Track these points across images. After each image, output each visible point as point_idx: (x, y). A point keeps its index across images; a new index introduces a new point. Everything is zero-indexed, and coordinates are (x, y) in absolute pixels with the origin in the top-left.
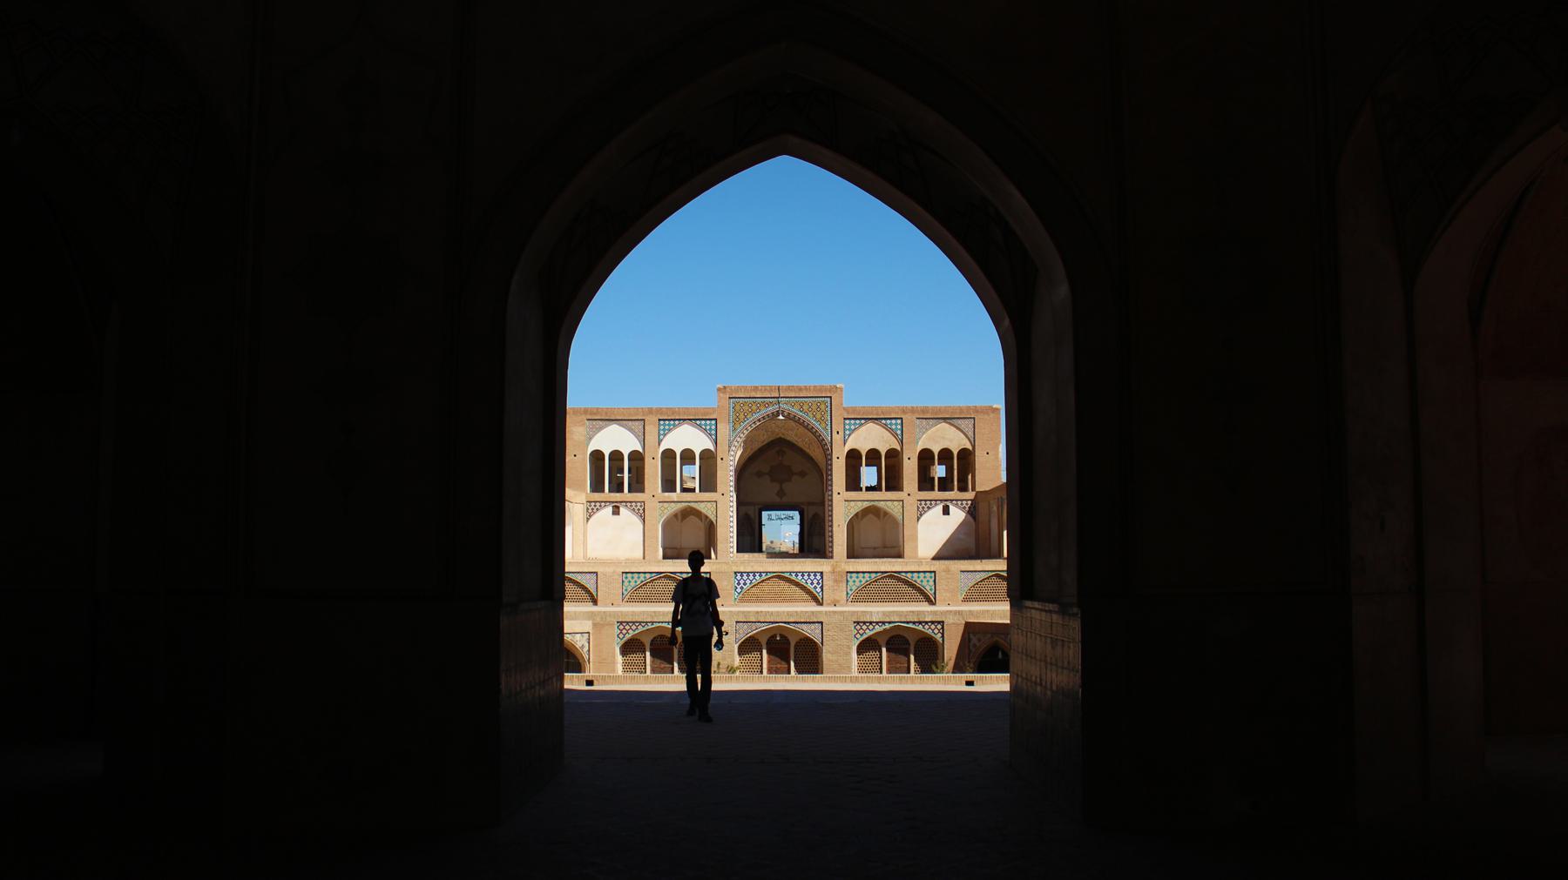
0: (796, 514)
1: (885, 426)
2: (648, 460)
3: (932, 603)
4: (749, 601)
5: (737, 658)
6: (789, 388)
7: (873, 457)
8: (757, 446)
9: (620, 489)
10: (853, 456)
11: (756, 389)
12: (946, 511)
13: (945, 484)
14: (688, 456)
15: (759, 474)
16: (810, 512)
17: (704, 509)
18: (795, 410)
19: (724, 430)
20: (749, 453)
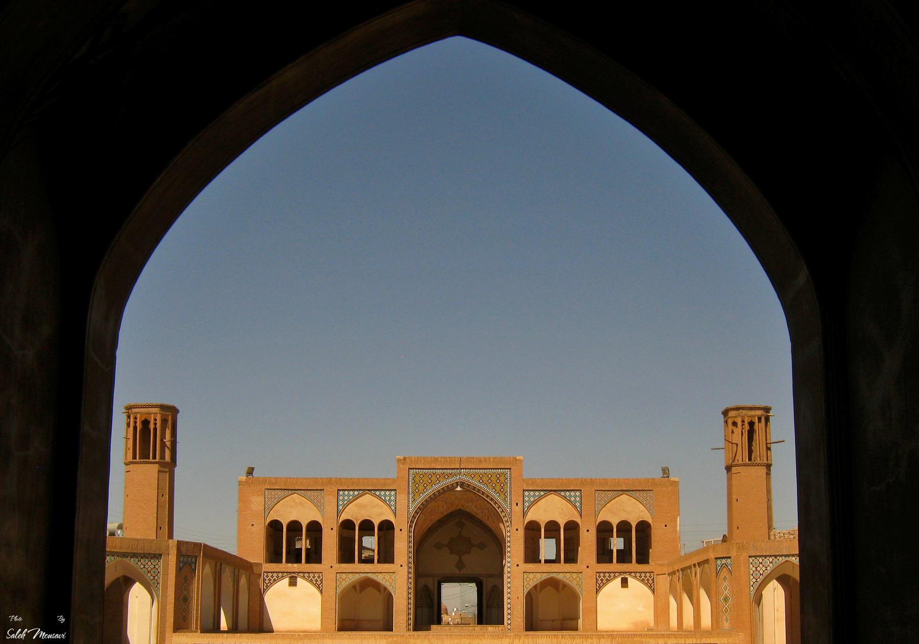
0: (474, 585)
1: (565, 497)
6: (469, 460)
7: (552, 529)
9: (298, 561)
10: (532, 530)
11: (436, 460)
12: (624, 583)
13: (624, 557)
14: (367, 527)
15: (439, 546)
16: (488, 584)
18: (475, 482)
19: (402, 499)
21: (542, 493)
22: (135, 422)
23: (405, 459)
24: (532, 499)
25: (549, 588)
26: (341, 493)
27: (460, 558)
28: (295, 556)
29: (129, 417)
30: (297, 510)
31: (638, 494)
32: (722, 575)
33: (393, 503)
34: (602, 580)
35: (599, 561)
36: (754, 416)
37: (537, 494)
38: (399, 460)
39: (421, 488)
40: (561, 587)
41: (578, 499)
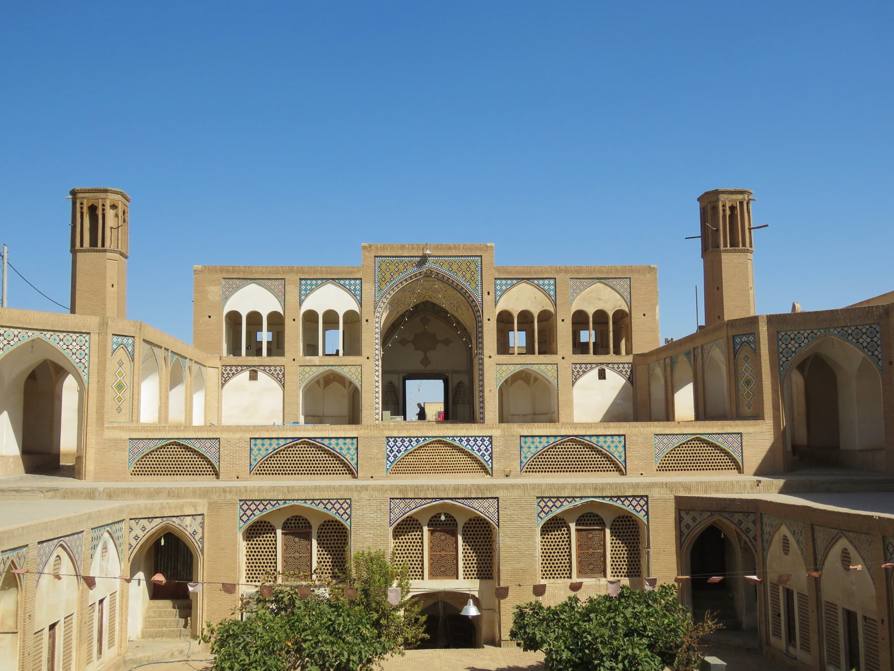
1: (538, 287)
2: (288, 322)
3: (622, 473)
4: (403, 472)
5: (392, 543)
7: (525, 318)
8: (402, 309)
10: (504, 320)
11: (403, 247)
12: (602, 375)
13: (601, 347)
14: (331, 319)
15: (403, 342)
16: (454, 380)
17: (348, 373)
18: (444, 270)
19: (369, 289)
20: (395, 316)
21: (515, 282)
22: (82, 208)
23: (370, 246)
24: (504, 288)
25: (520, 382)
26: (303, 282)
27: (425, 354)
28: (255, 349)
29: (74, 203)
30: (254, 299)
31: (615, 282)
32: (741, 356)
33: (358, 293)
34: (578, 372)
35: (574, 353)
36: (735, 201)
37: (509, 282)
38: (364, 248)
39: (388, 276)
40: (532, 381)
41: (552, 287)
